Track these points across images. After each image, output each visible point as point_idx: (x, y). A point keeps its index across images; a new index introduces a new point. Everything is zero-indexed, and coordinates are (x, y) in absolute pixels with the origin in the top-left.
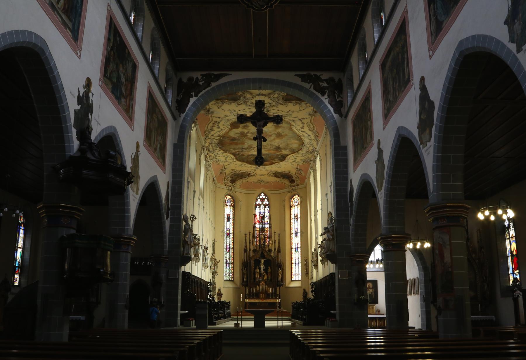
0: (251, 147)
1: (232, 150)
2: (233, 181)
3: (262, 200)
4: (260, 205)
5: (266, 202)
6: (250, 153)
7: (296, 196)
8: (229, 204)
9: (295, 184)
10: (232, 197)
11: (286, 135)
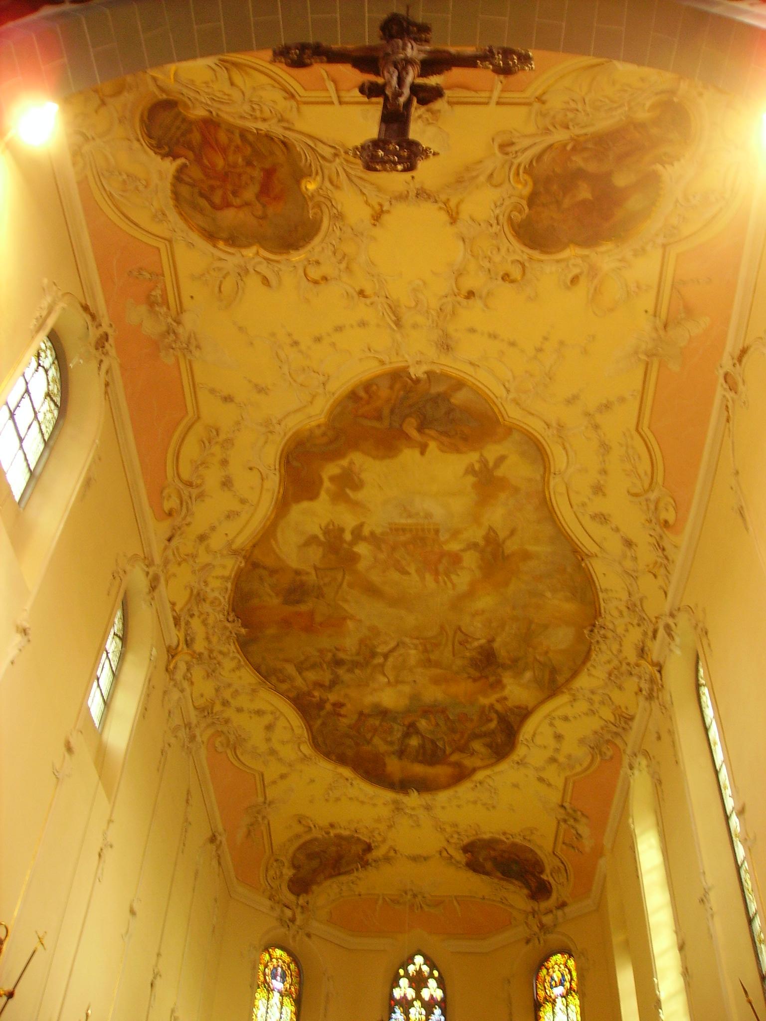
0: (373, 655)
1: (291, 669)
2: (301, 885)
3: (418, 982)
4: (406, 1005)
5: (432, 990)
6: (369, 699)
7: (558, 958)
8: (277, 984)
9: (552, 902)
10: (295, 960)
11: (526, 556)
